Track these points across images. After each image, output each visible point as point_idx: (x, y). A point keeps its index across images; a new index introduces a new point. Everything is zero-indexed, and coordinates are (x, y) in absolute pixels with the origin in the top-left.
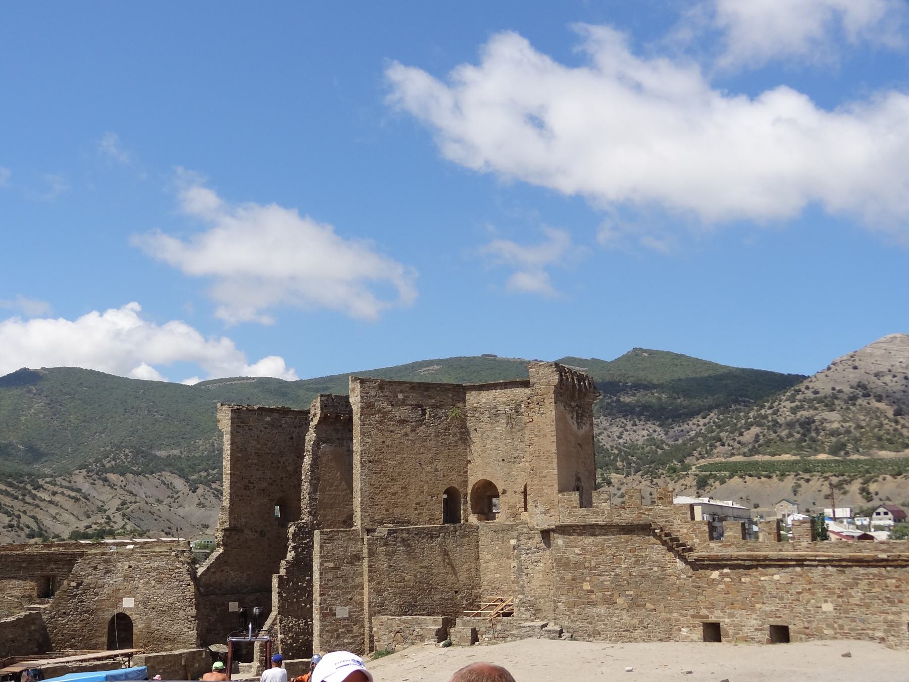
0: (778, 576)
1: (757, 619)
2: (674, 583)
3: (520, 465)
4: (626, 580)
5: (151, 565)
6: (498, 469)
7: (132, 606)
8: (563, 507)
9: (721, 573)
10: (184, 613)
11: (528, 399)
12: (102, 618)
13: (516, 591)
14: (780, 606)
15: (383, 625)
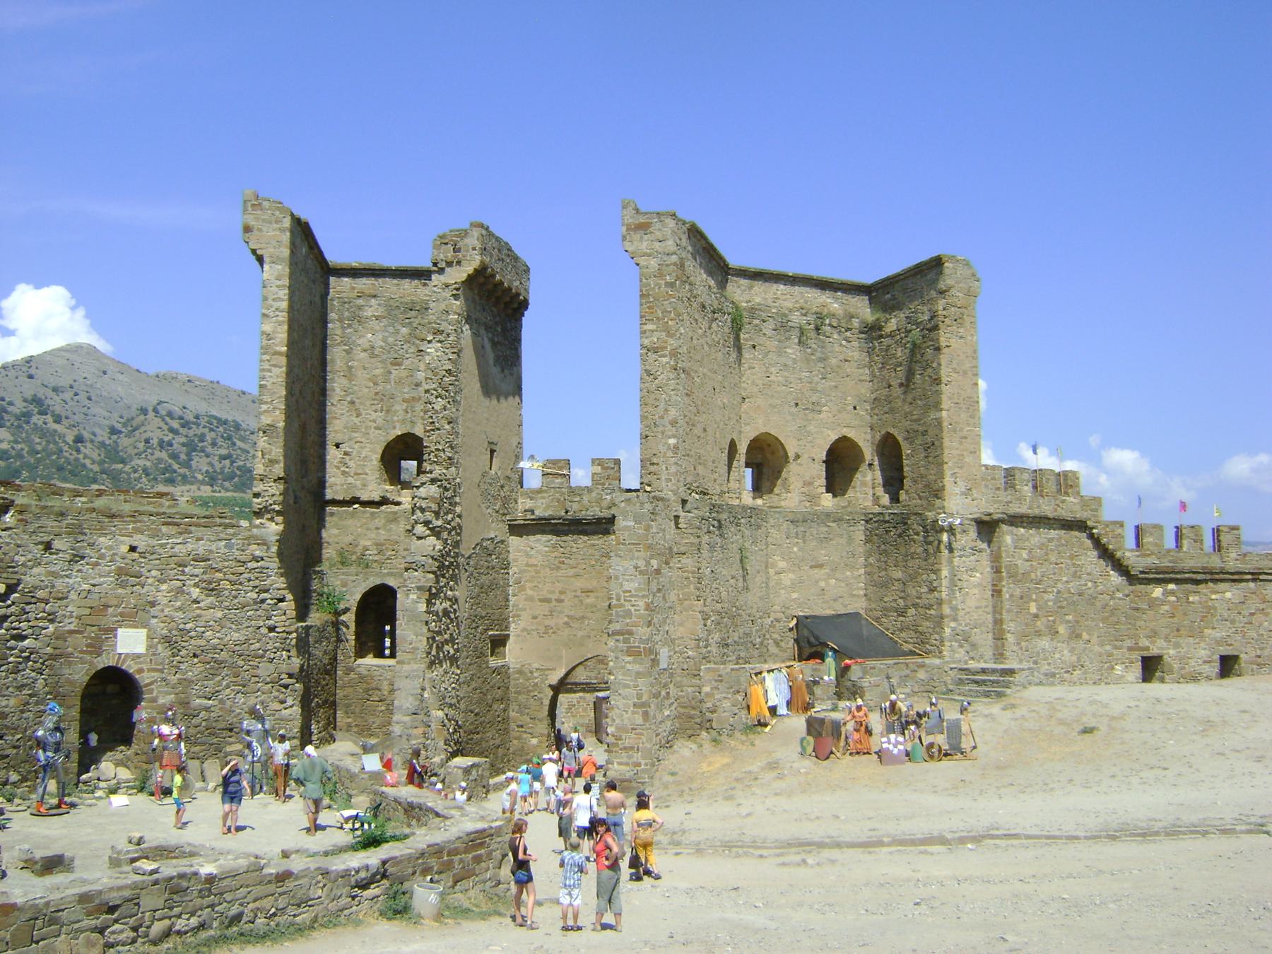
0: (1230, 593)
1: (1205, 649)
2: (1107, 605)
3: (821, 416)
4: (1066, 599)
5: (190, 547)
6: (790, 418)
7: (141, 649)
8: (986, 486)
9: (1165, 590)
10: (271, 667)
11: (944, 309)
12: (68, 681)
13: (947, 616)
14: (1231, 631)
15: (721, 681)
